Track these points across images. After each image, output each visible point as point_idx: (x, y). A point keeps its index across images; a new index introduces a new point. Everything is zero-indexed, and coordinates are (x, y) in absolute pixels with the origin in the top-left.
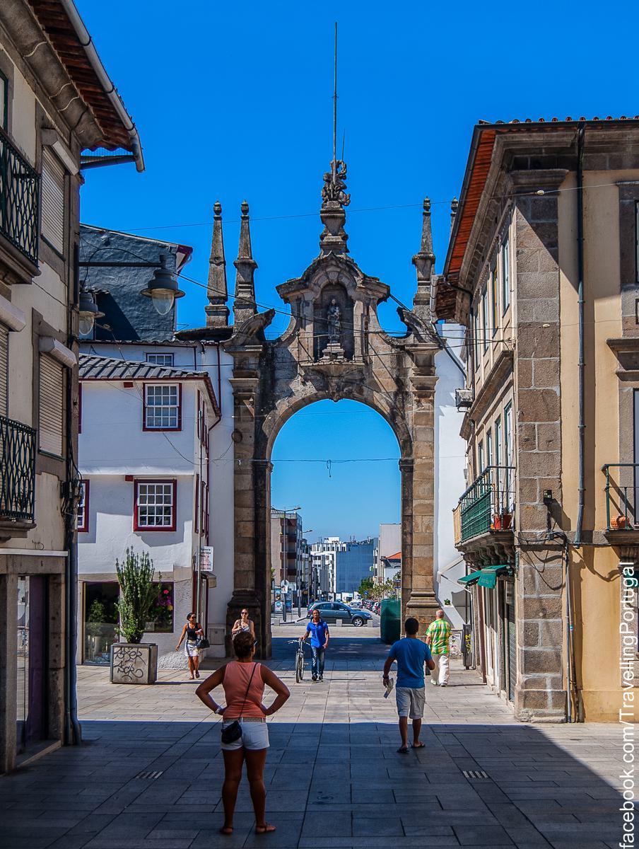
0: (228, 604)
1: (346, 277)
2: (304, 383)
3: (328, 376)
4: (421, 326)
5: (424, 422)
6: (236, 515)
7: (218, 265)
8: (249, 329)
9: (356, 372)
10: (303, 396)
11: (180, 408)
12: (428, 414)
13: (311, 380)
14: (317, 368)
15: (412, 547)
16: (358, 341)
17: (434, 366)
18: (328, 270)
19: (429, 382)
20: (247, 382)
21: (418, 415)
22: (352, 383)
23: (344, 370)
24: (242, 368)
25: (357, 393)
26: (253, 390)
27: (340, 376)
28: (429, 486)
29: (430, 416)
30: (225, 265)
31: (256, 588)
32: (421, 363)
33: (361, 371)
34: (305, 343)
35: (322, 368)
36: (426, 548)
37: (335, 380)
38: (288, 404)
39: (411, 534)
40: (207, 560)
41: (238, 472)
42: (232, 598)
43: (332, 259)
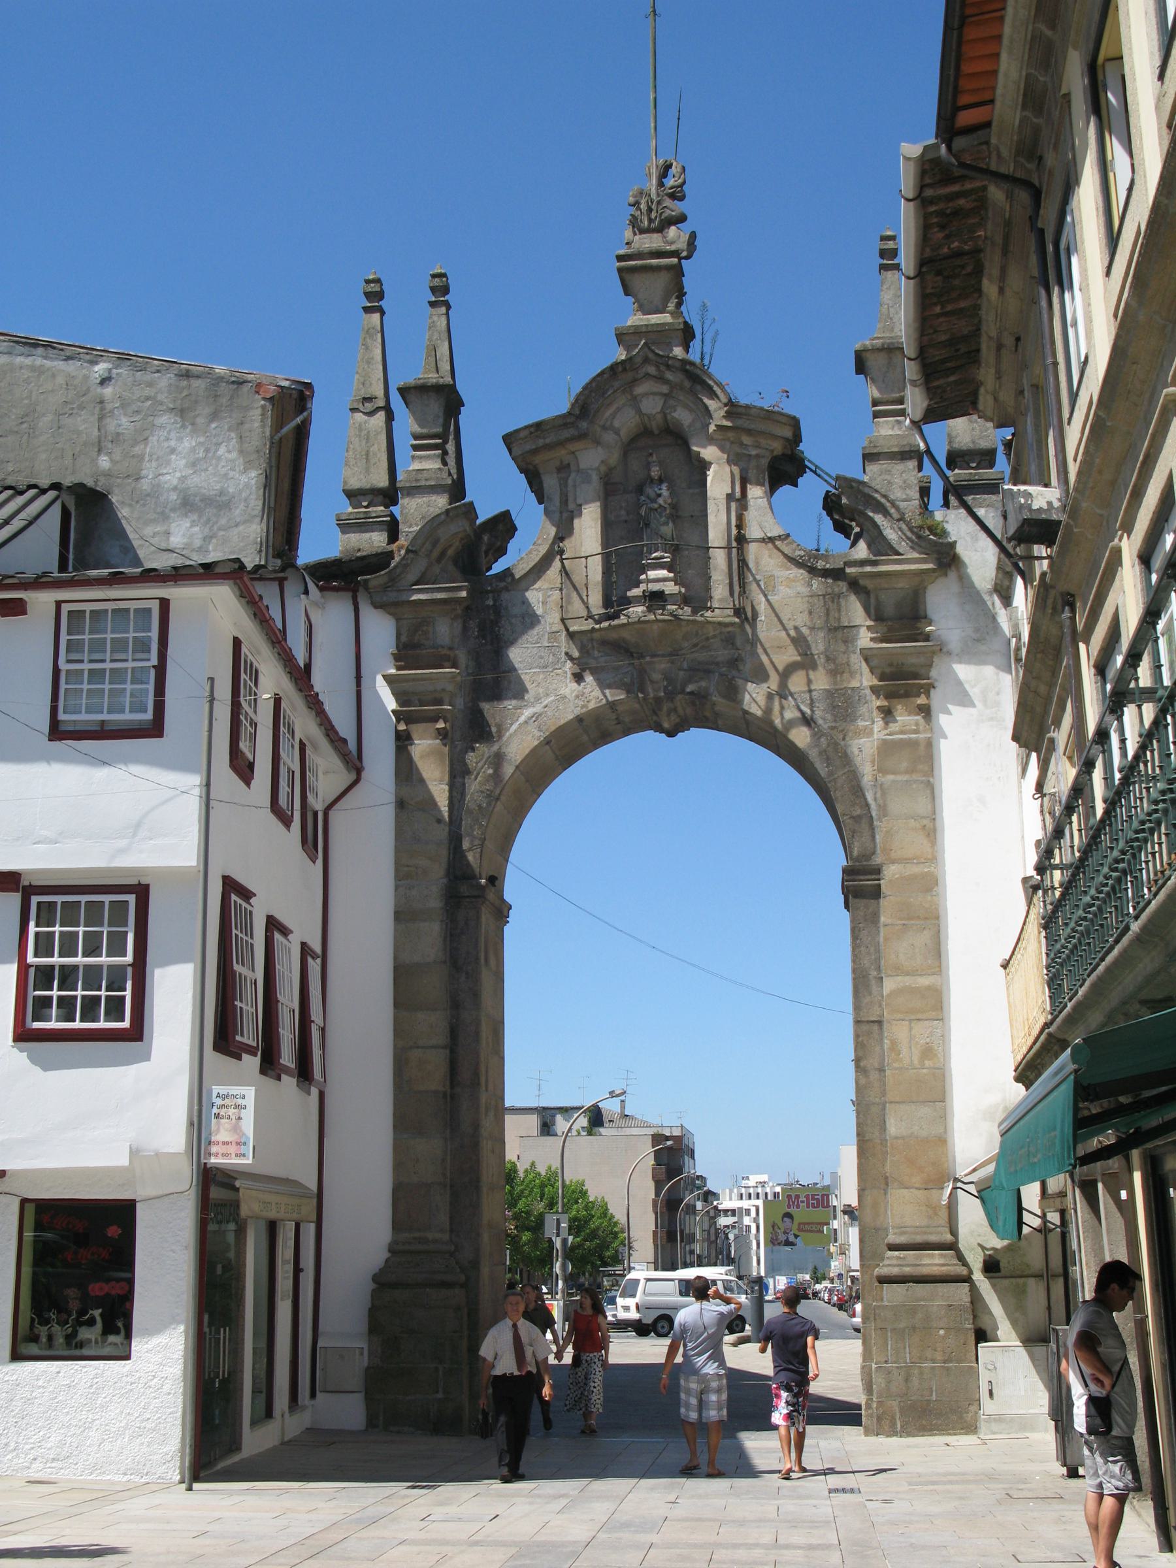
0: (375, 1278)
1: (686, 407)
2: (578, 678)
4: (886, 513)
5: (904, 765)
6: (400, 1031)
7: (371, 414)
8: (435, 543)
10: (578, 711)
11: (161, 670)
12: (913, 744)
13: (594, 672)
14: (614, 635)
15: (884, 1109)
16: (719, 559)
17: (926, 617)
18: (639, 390)
19: (913, 660)
20: (430, 678)
21: (887, 749)
22: (708, 672)
25: (724, 697)
26: (447, 700)
27: (674, 653)
28: (925, 937)
29: (922, 748)
30: (390, 417)
31: (451, 1231)
32: (889, 610)
33: (729, 640)
34: (577, 571)
35: (625, 634)
36: (925, 1111)
37: (662, 665)
38: (537, 734)
39: (882, 1070)
40: (236, 1129)
41: (403, 916)
42: (387, 1261)
43: (646, 360)
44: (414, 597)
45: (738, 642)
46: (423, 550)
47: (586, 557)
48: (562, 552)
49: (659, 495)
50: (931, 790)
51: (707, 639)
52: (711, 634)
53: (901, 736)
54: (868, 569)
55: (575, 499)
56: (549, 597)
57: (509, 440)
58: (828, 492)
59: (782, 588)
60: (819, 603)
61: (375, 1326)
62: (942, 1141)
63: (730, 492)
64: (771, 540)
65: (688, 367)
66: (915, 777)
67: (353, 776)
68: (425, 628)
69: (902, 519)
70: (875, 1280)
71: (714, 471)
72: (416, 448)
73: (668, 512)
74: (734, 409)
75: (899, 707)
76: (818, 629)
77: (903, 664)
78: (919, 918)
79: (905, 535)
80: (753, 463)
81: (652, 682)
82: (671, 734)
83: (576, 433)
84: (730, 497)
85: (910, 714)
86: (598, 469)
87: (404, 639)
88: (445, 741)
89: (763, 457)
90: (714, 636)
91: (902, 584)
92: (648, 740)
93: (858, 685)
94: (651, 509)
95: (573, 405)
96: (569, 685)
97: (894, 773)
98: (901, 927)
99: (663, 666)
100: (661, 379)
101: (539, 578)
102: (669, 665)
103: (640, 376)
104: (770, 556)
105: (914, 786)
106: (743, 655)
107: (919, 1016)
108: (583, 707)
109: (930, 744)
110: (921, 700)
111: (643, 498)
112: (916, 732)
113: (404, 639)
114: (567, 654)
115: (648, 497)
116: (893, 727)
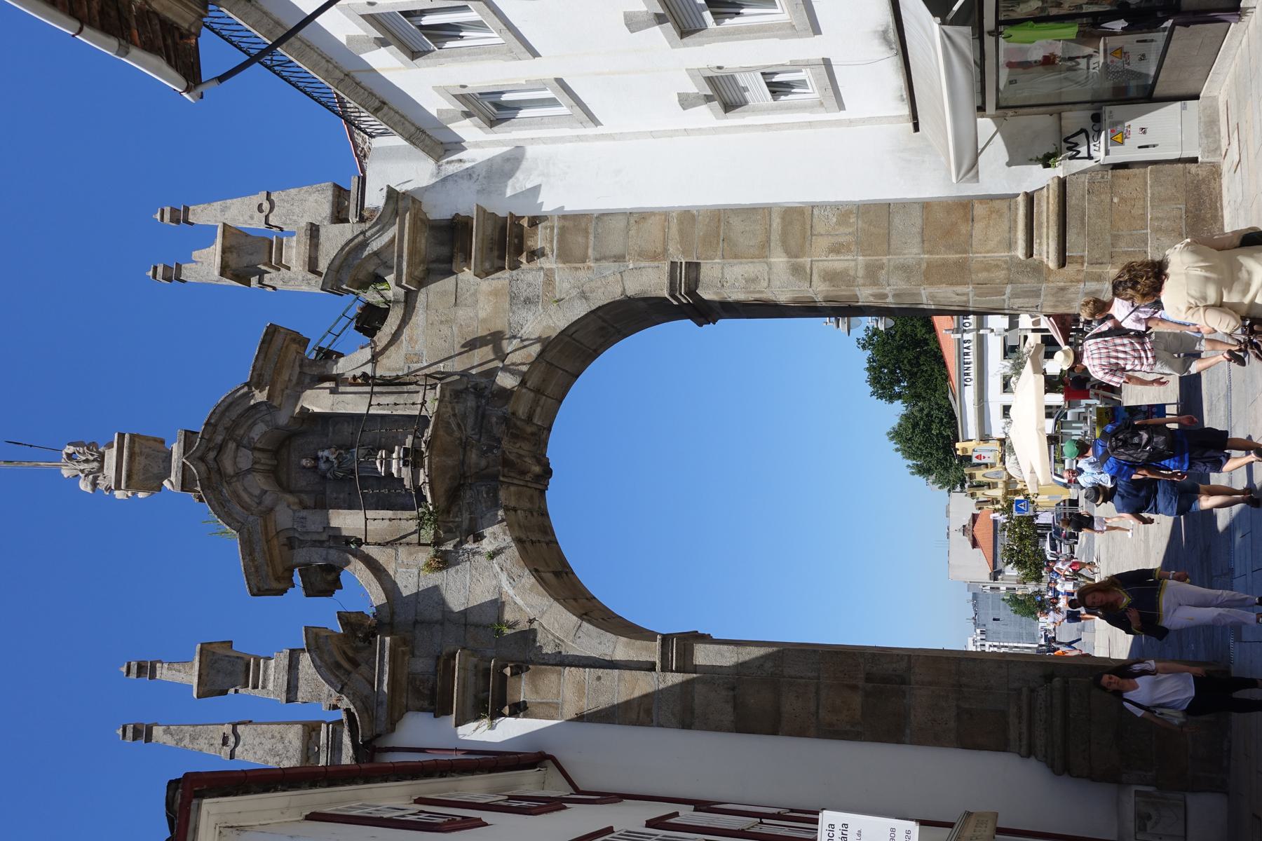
1: (251, 427)
3: (463, 476)
5: (581, 239)
6: (800, 732)
8: (338, 666)
9: (459, 408)
12: (563, 231)
18: (230, 470)
22: (483, 416)
23: (450, 433)
24: (433, 690)
25: (507, 403)
28: (736, 222)
29: (566, 224)
32: (444, 251)
36: (897, 221)
37: (473, 456)
44: (385, 689)
45: (461, 387)
46: (343, 678)
47: (367, 519)
48: (359, 542)
49: (327, 458)
50: (603, 216)
51: (455, 415)
52: (449, 409)
53: (555, 242)
55: (318, 533)
56: (403, 562)
58: (357, 328)
59: (417, 347)
61: (1110, 776)
62: (926, 205)
63: (328, 390)
65: (212, 421)
66: (591, 230)
67: (549, 763)
68: (418, 683)
70: (1061, 270)
71: (309, 404)
72: (255, 687)
73: (343, 452)
74: (257, 381)
75: (529, 243)
77: (492, 239)
78: (718, 227)
81: (487, 467)
82: (548, 473)
84: (333, 391)
85: (536, 234)
86: (294, 511)
87: (426, 704)
88: (524, 668)
90: (453, 409)
91: (422, 243)
92: (556, 498)
94: (338, 467)
97: (587, 248)
98: (725, 244)
99: (474, 456)
100: (221, 448)
101: (385, 570)
102: (474, 451)
103: (216, 466)
104: (389, 358)
105: (600, 231)
106: (473, 383)
107: (808, 227)
108: (505, 533)
109: (564, 217)
110: (525, 223)
111: (328, 475)
112: (552, 228)
113: (426, 704)
115: (329, 470)
116: (548, 250)
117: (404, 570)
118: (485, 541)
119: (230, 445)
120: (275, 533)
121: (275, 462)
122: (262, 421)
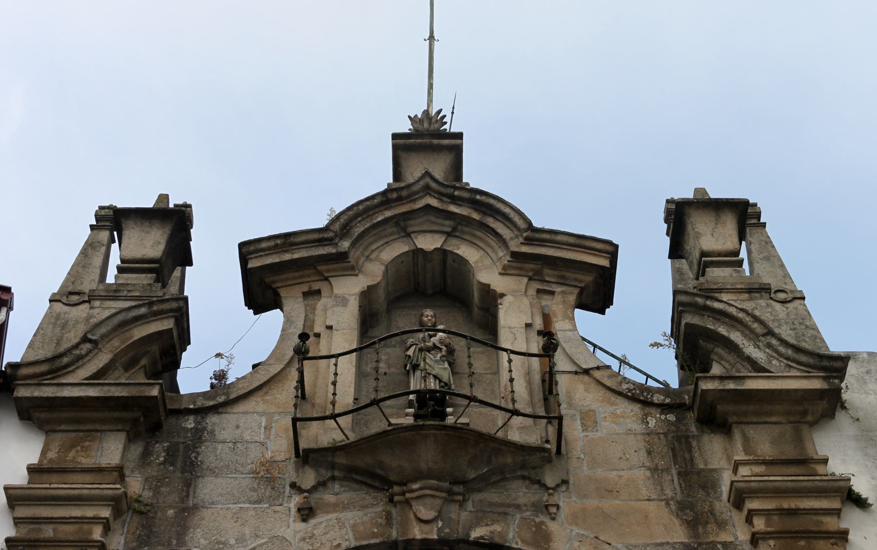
54: (731, 386)
57: (247, 250)
60: (661, 446)
64: (587, 372)
65: (478, 197)
68: (87, 444)
69: (770, 333)
76: (663, 470)
79: (776, 351)
80: (558, 298)
83: (334, 251)
89: (571, 293)
93: (730, 539)
95: (333, 221)
96: (292, 524)
114: (293, 485)
117: (263, 424)
118: (302, 526)
119: (447, 222)
120: (326, 275)
121: (430, 292)
122: (481, 257)
